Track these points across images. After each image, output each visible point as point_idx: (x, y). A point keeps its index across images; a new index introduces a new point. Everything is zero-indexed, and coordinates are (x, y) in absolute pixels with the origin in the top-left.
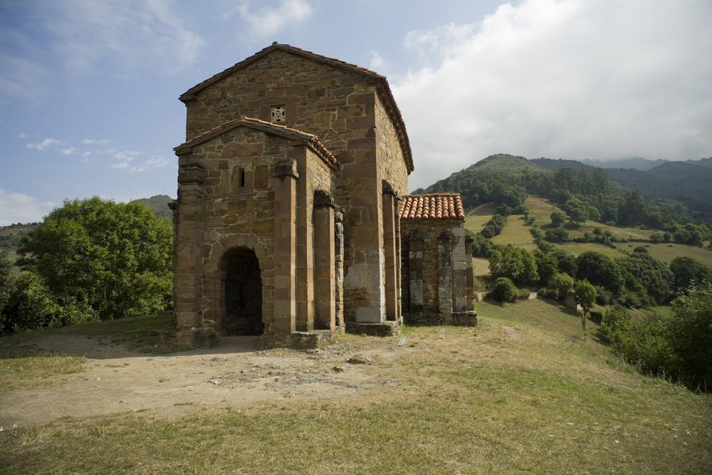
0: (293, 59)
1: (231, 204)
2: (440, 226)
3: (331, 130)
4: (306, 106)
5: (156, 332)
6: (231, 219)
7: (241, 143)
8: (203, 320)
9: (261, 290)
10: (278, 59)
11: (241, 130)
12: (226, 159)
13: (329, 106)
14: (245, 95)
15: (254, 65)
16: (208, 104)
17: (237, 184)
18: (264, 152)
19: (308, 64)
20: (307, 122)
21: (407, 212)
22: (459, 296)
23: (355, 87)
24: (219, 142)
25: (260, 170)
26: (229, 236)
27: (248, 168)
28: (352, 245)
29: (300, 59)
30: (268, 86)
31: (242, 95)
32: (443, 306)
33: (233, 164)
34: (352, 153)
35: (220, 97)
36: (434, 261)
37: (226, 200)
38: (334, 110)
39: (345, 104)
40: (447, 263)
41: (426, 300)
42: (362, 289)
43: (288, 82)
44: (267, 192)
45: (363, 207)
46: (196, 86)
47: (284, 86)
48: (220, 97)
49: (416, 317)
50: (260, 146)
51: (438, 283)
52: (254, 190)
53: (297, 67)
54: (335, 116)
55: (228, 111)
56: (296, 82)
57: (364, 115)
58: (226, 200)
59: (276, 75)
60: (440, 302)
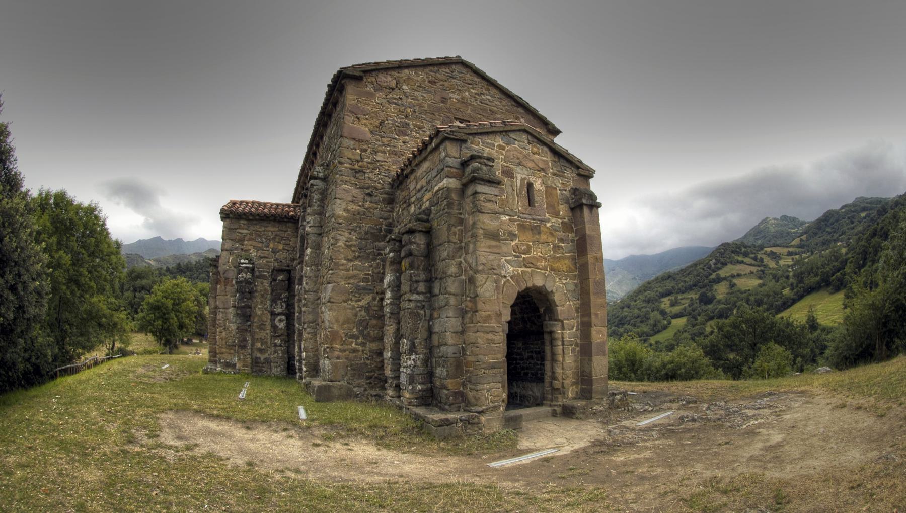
1: (522, 227)
5: (447, 420)
15: (436, 69)
16: (376, 90)
19: (493, 91)
24: (499, 141)
27: (538, 185)
30: (451, 95)
33: (520, 175)
35: (394, 86)
43: (473, 100)
48: (394, 86)
50: (546, 162)
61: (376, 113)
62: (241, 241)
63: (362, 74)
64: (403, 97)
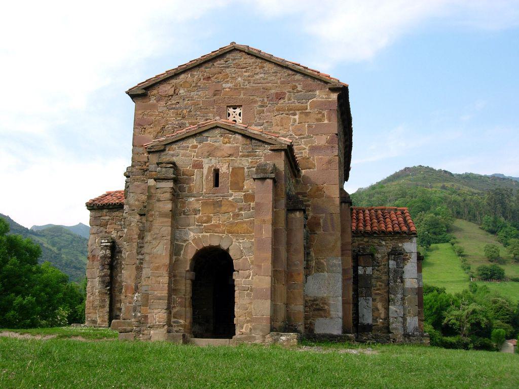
0: (253, 60)
1: (205, 204)
3: (291, 135)
4: (265, 109)
6: (205, 218)
7: (217, 144)
8: (173, 320)
10: (235, 59)
11: (217, 131)
12: (200, 159)
13: (289, 110)
14: (199, 93)
16: (158, 101)
17: (212, 184)
18: (240, 154)
19: (267, 66)
20: (266, 125)
21: (354, 224)
22: (410, 316)
23: (317, 92)
24: (194, 142)
25: (236, 172)
26: (203, 236)
27: (224, 169)
28: (312, 254)
29: (259, 60)
30: (224, 85)
31: (195, 93)
32: (394, 325)
34: (314, 161)
35: (171, 92)
36: (384, 277)
37: (199, 200)
38: (295, 114)
39: (307, 109)
40: (399, 280)
41: (375, 320)
42: (322, 299)
43: (246, 83)
45: (324, 215)
46: (146, 81)
47: (242, 86)
48: (171, 92)
49: (364, 338)
51: (389, 301)
52: (230, 192)
53: (255, 68)
54: (296, 121)
55: (180, 108)
56: (254, 83)
57: (326, 122)
58: (199, 200)
59: (234, 76)
60: (391, 322)
61: (159, 121)
62: (105, 225)
63: (144, 91)
64: (181, 101)
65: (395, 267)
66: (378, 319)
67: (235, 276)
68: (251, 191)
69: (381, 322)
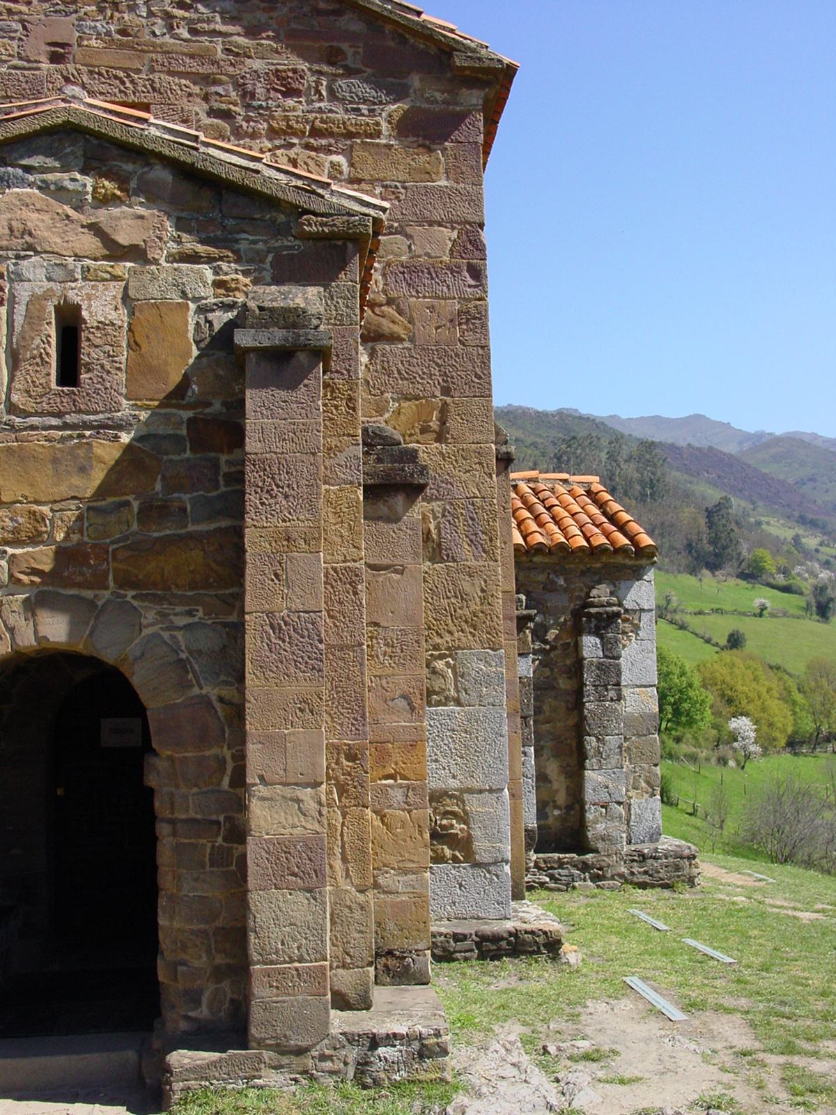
2: (583, 573)
9: (153, 840)
27: (101, 307)
32: (600, 827)
40: (612, 694)
44: (187, 414)
65: (601, 654)
66: (547, 810)
67: (157, 775)
68: (217, 407)
69: (556, 818)
